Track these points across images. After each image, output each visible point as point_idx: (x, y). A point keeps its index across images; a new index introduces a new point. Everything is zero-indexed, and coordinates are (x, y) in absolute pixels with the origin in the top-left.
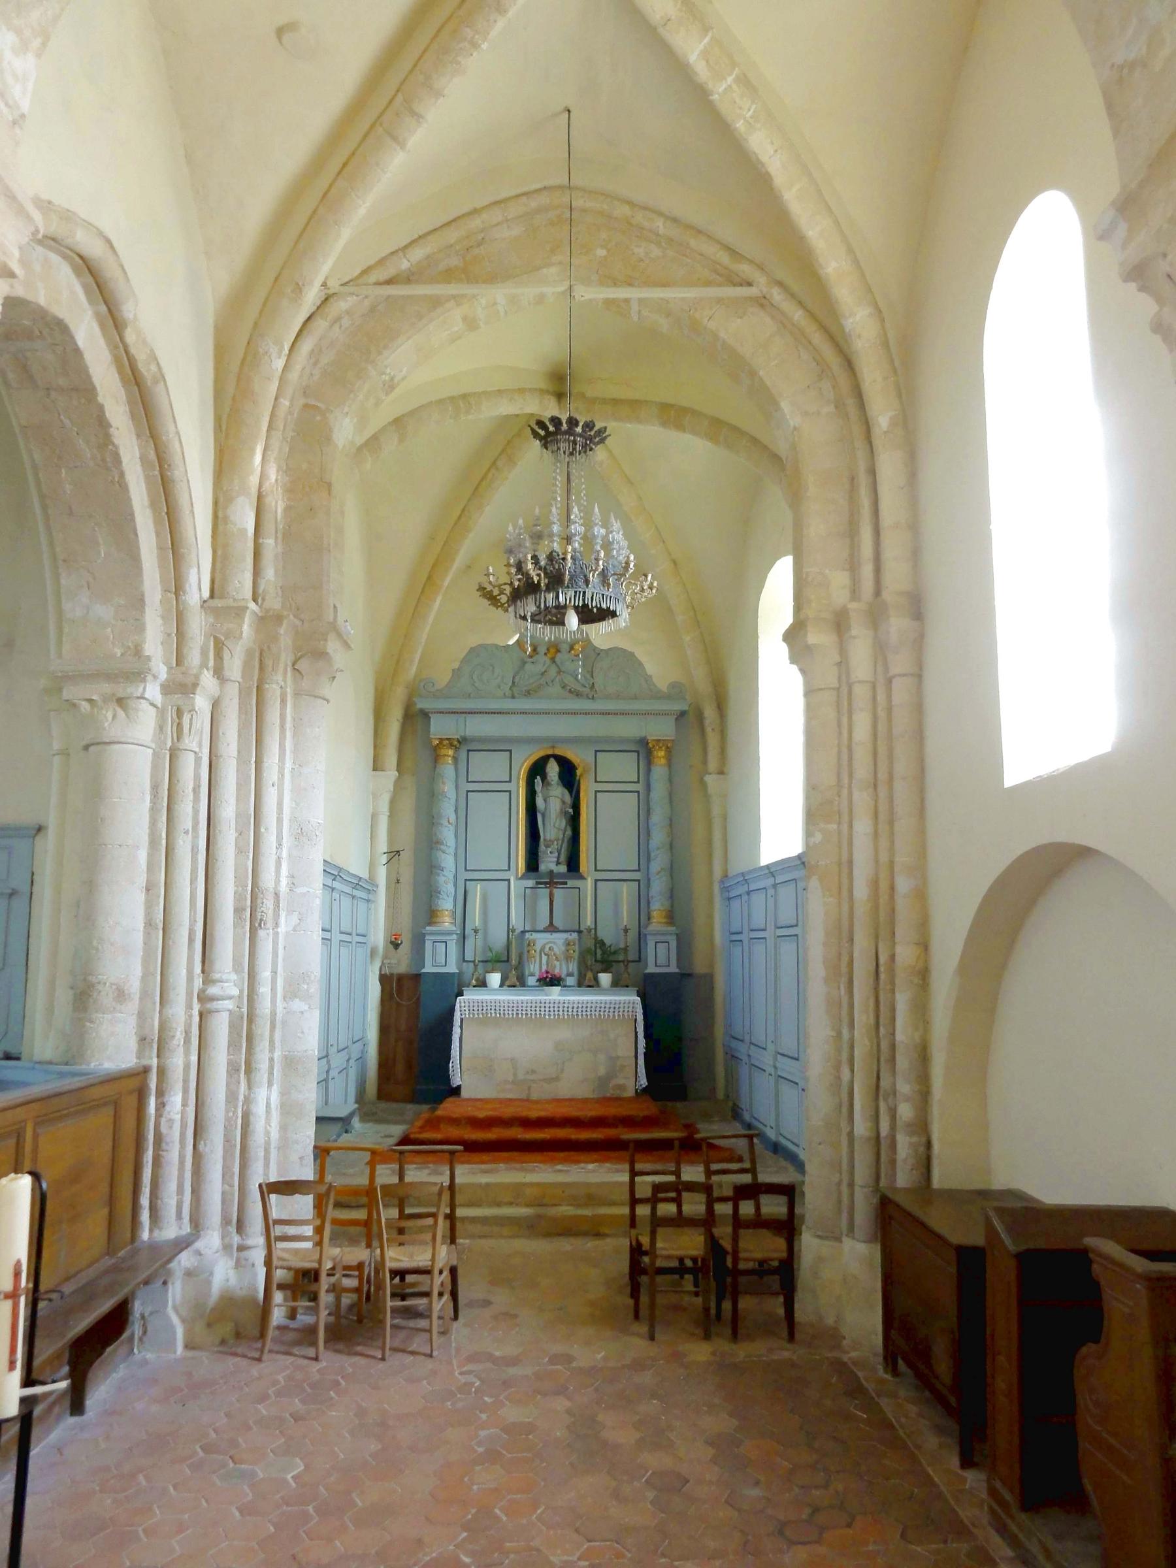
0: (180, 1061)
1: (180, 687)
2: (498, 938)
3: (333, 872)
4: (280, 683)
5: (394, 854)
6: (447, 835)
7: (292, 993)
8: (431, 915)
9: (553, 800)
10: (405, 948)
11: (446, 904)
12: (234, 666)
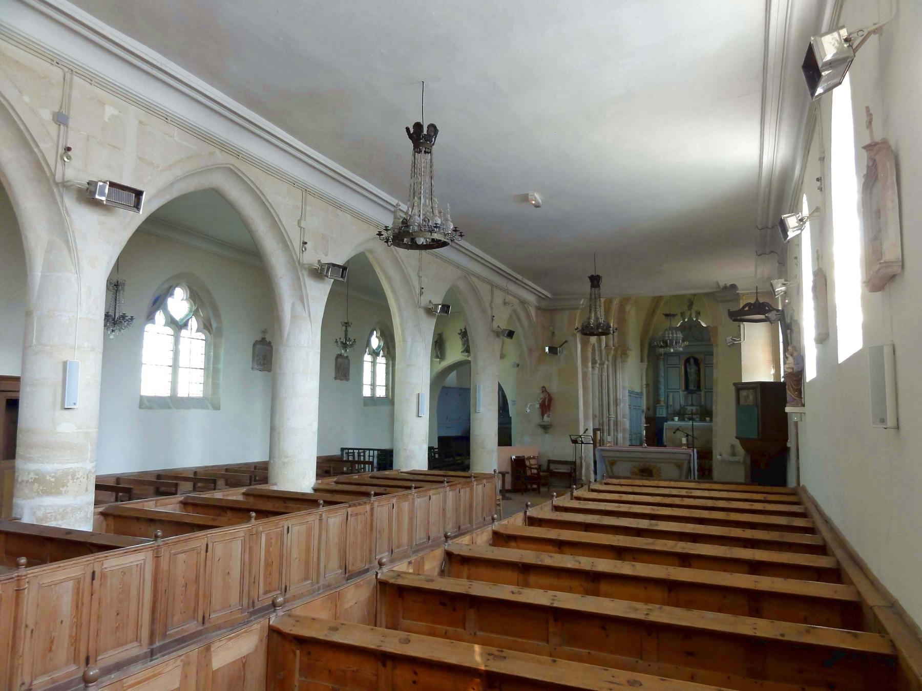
0: (606, 428)
1: (602, 364)
2: (678, 407)
3: (631, 392)
4: (619, 361)
5: (647, 385)
6: (662, 380)
7: (624, 417)
8: (658, 401)
9: (692, 369)
10: (652, 409)
11: (662, 398)
12: (610, 359)
